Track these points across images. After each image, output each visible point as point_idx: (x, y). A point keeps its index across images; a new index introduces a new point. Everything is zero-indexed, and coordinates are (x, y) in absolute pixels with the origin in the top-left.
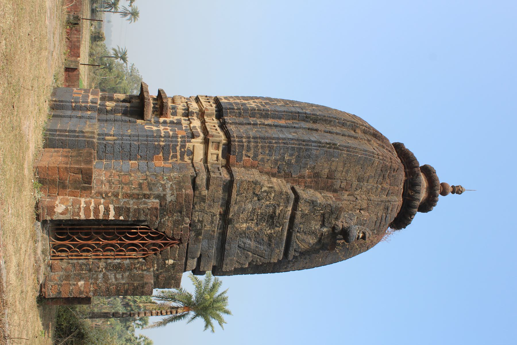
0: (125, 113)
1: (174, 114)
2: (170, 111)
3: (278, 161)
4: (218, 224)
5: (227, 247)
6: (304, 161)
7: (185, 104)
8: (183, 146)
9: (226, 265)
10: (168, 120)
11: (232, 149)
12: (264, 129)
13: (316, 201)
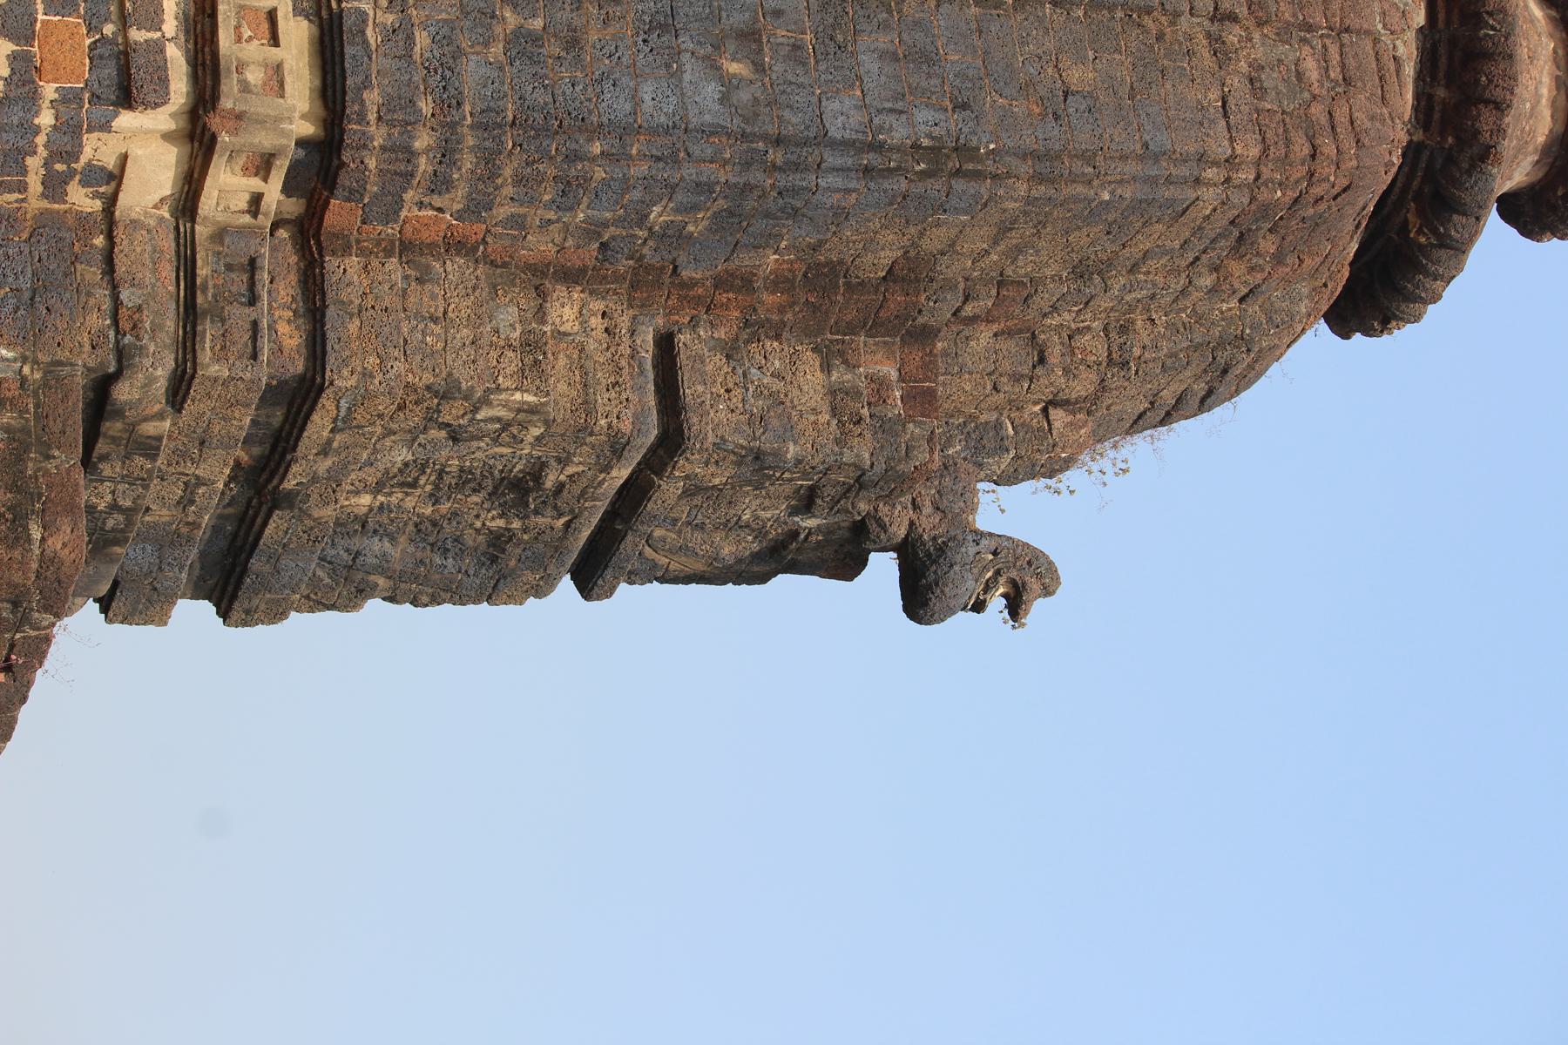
3: (605, 225)
4: (223, 493)
5: (255, 564)
6: (760, 225)
8: (55, 155)
9: (247, 612)
11: (344, 179)
13: (776, 454)
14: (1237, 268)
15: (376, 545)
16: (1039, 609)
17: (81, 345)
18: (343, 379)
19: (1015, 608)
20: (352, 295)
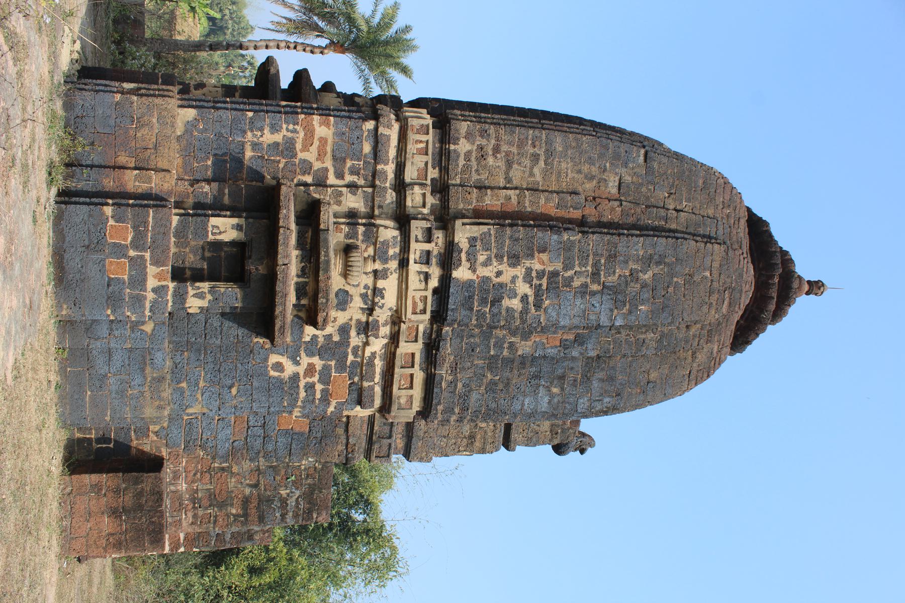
7: (369, 281)
12: (507, 374)
19: (582, 451)
20: (421, 434)
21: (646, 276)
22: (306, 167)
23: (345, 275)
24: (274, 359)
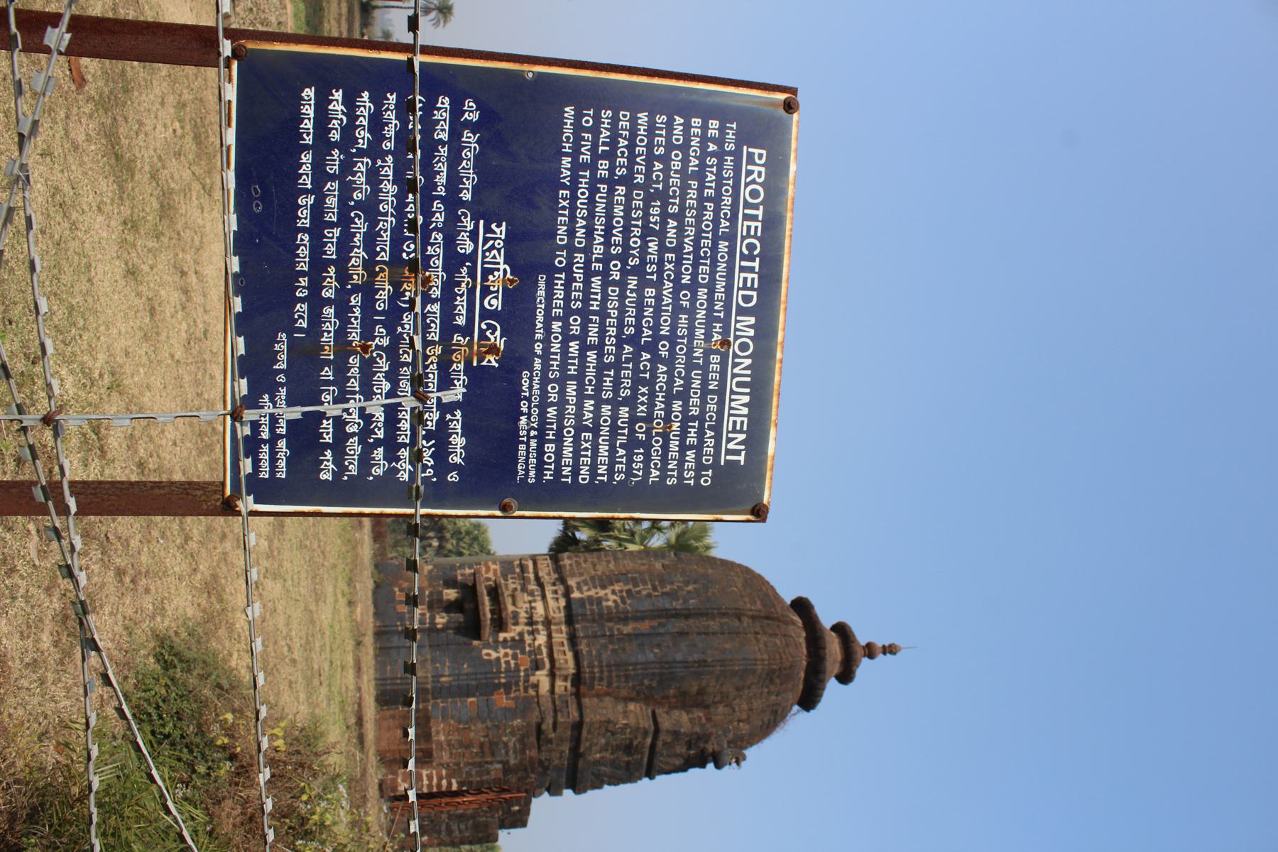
0: (459, 630)
1: (516, 624)
2: (510, 621)
10: (508, 635)
14: (772, 688)
15: (603, 768)
16: (743, 764)
17: (534, 717)
18: (587, 720)
19: (738, 762)
21: (690, 588)
22: (488, 579)
23: (514, 604)
24: (485, 651)
